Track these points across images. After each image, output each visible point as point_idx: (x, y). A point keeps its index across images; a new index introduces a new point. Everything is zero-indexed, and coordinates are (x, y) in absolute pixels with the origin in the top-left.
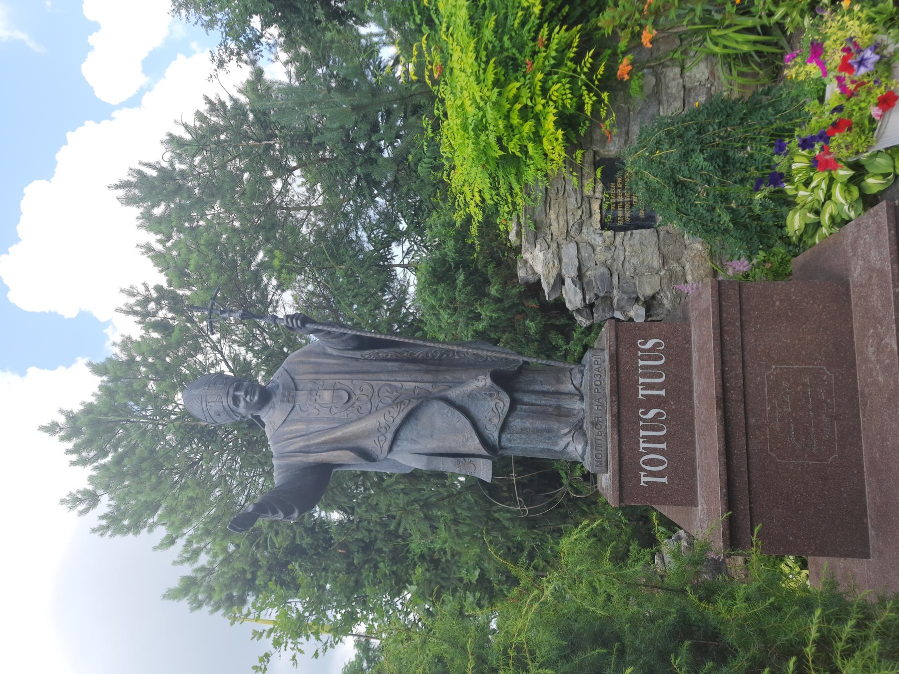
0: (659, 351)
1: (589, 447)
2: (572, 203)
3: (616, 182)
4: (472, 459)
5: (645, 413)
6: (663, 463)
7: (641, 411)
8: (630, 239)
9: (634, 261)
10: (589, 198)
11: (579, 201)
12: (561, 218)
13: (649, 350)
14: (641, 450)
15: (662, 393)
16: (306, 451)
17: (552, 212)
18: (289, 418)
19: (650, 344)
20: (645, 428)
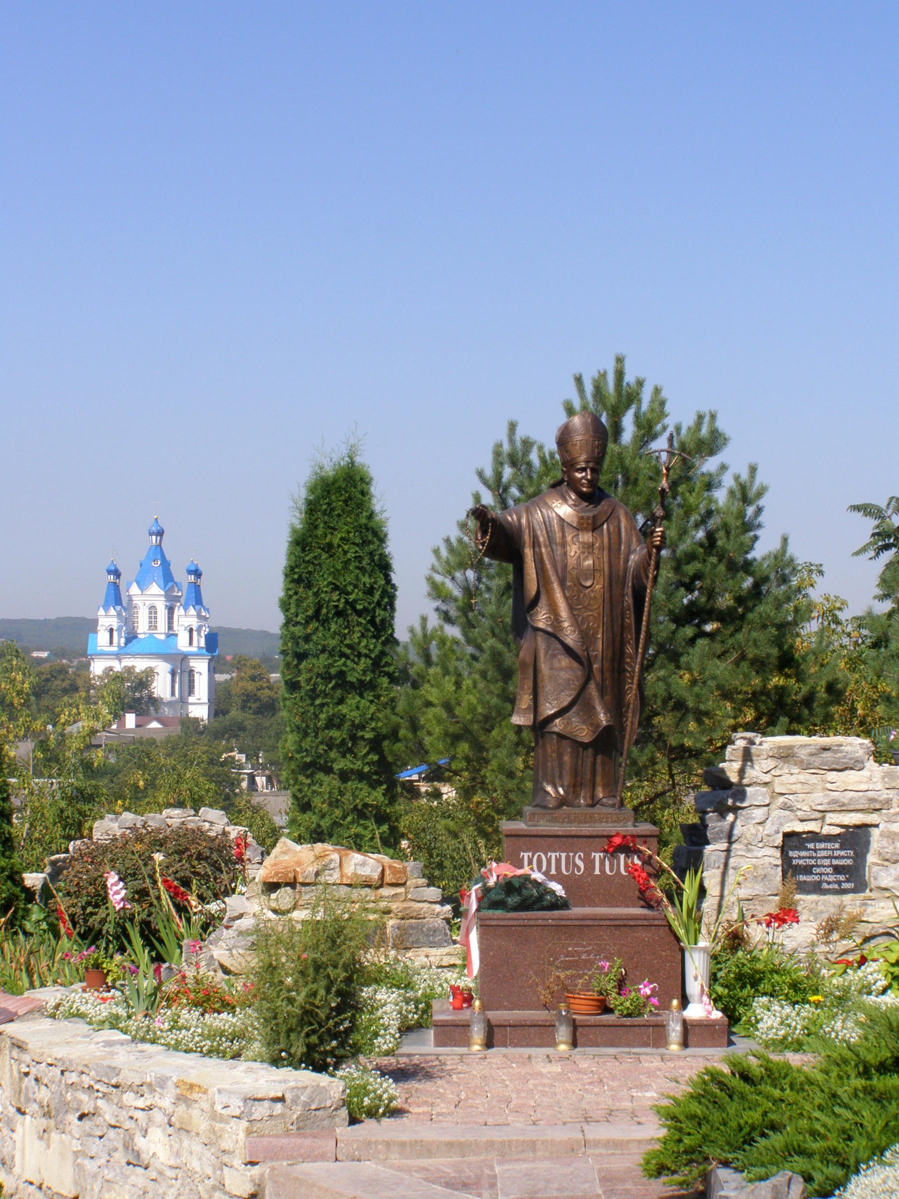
3: (841, 849)
5: (580, 857)
11: (819, 808)
12: (799, 786)
15: (597, 872)
16: (535, 543)
17: (808, 776)
20: (567, 858)
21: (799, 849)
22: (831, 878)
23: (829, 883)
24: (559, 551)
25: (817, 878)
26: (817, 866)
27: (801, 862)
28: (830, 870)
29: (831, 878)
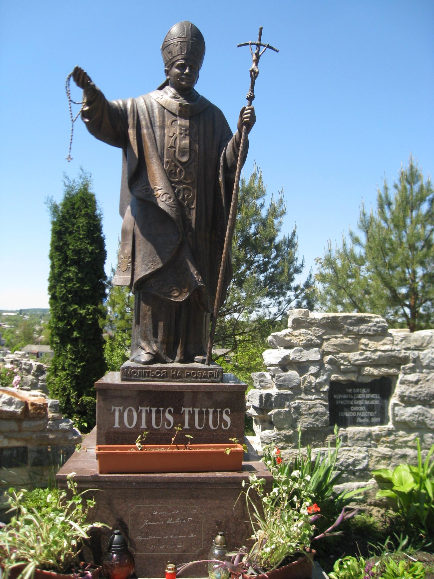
0: (221, 425)
1: (142, 366)
4: (131, 269)
6: (130, 424)
7: (172, 409)
8: (321, 404)
13: (221, 417)
14: (140, 408)
18: (166, 110)
19: (225, 417)
21: (342, 393)
22: (365, 414)
23: (362, 418)
24: (158, 133)
25: (353, 414)
26: (354, 405)
27: (342, 402)
28: (363, 408)
29: (365, 414)
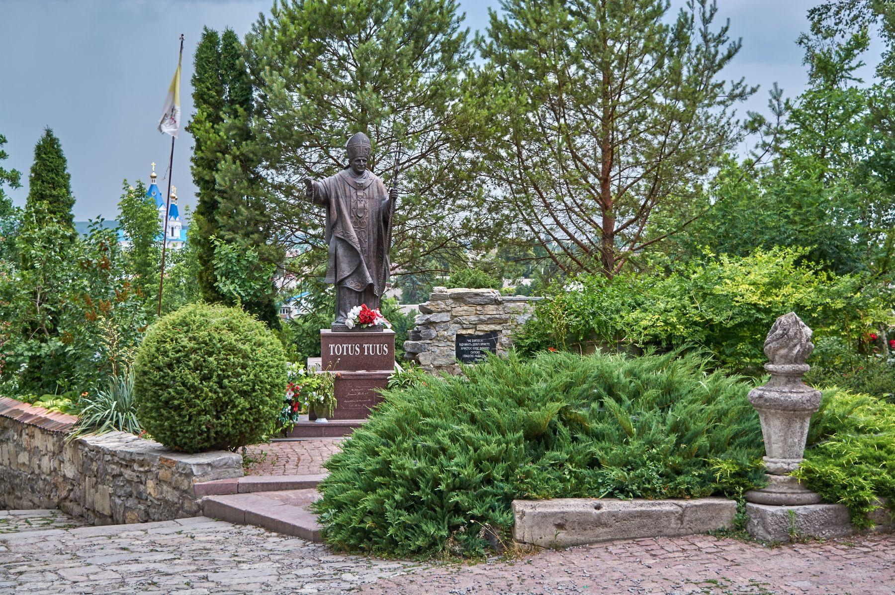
2: (473, 318)
9: (438, 352)
10: (476, 328)
16: (337, 197)
